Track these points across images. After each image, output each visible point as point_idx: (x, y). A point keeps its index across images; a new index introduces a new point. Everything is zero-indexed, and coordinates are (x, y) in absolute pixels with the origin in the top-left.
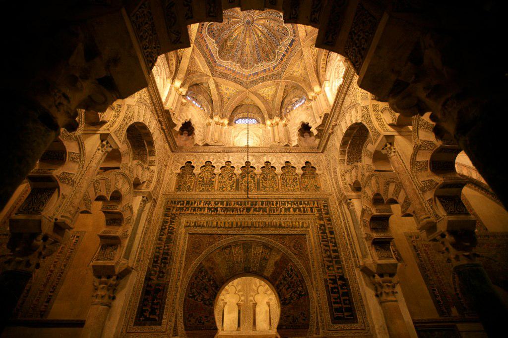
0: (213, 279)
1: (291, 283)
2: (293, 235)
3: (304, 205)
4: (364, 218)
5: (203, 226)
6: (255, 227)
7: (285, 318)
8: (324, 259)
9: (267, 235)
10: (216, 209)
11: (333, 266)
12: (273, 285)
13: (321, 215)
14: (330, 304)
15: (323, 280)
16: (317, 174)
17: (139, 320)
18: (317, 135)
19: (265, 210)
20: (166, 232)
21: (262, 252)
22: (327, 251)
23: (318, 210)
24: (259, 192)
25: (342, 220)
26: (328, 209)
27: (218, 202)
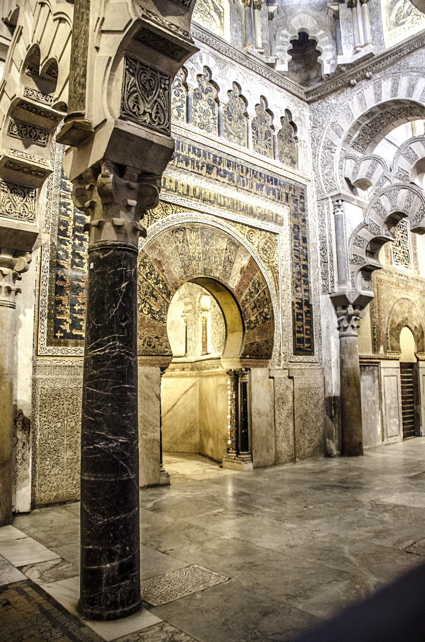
0: (163, 281)
1: (257, 301)
2: (264, 230)
3: (279, 187)
4: (358, 234)
8: (295, 275)
9: (234, 222)
14: (294, 333)
15: (291, 303)
16: (296, 138)
17: (56, 337)
18: (328, 75)
21: (226, 249)
24: (223, 139)
25: (318, 226)
26: (304, 202)
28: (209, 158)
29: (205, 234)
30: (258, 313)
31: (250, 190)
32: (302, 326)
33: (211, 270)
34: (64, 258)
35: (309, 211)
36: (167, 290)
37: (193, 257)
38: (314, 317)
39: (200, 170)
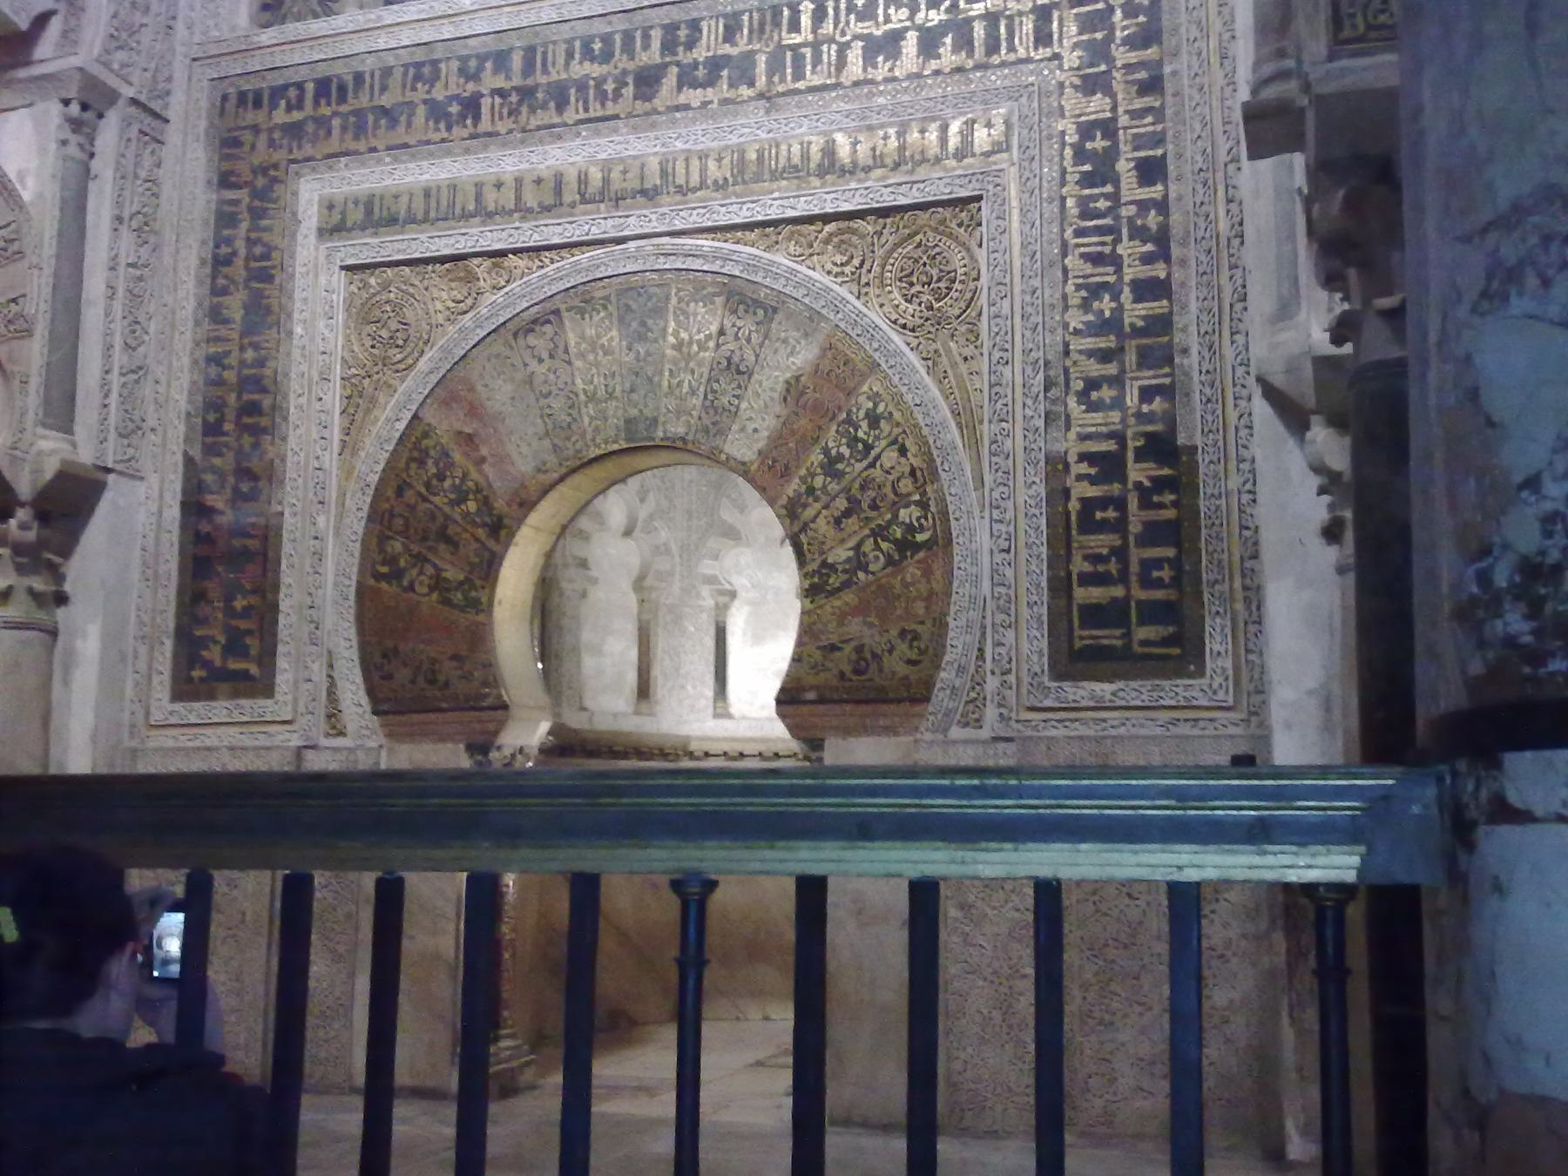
0: (478, 490)
1: (863, 488)
5: (412, 220)
6: (682, 191)
7: (818, 655)
8: (1077, 344)
10: (471, 106)
11: (1117, 381)
12: (771, 502)
13: (1099, 52)
14: (1060, 586)
15: (1042, 464)
17: (190, 680)
19: (743, 71)
20: (238, 270)
21: (721, 332)
22: (1096, 291)
23: (1087, 24)
27: (481, 59)
28: (646, 47)
29: (634, 306)
30: (867, 532)
31: (833, 81)
32: (1121, 553)
33: (655, 420)
34: (214, 488)
35: (1183, 30)
36: (490, 515)
37: (585, 391)
38: (1202, 505)
39: (609, 104)
